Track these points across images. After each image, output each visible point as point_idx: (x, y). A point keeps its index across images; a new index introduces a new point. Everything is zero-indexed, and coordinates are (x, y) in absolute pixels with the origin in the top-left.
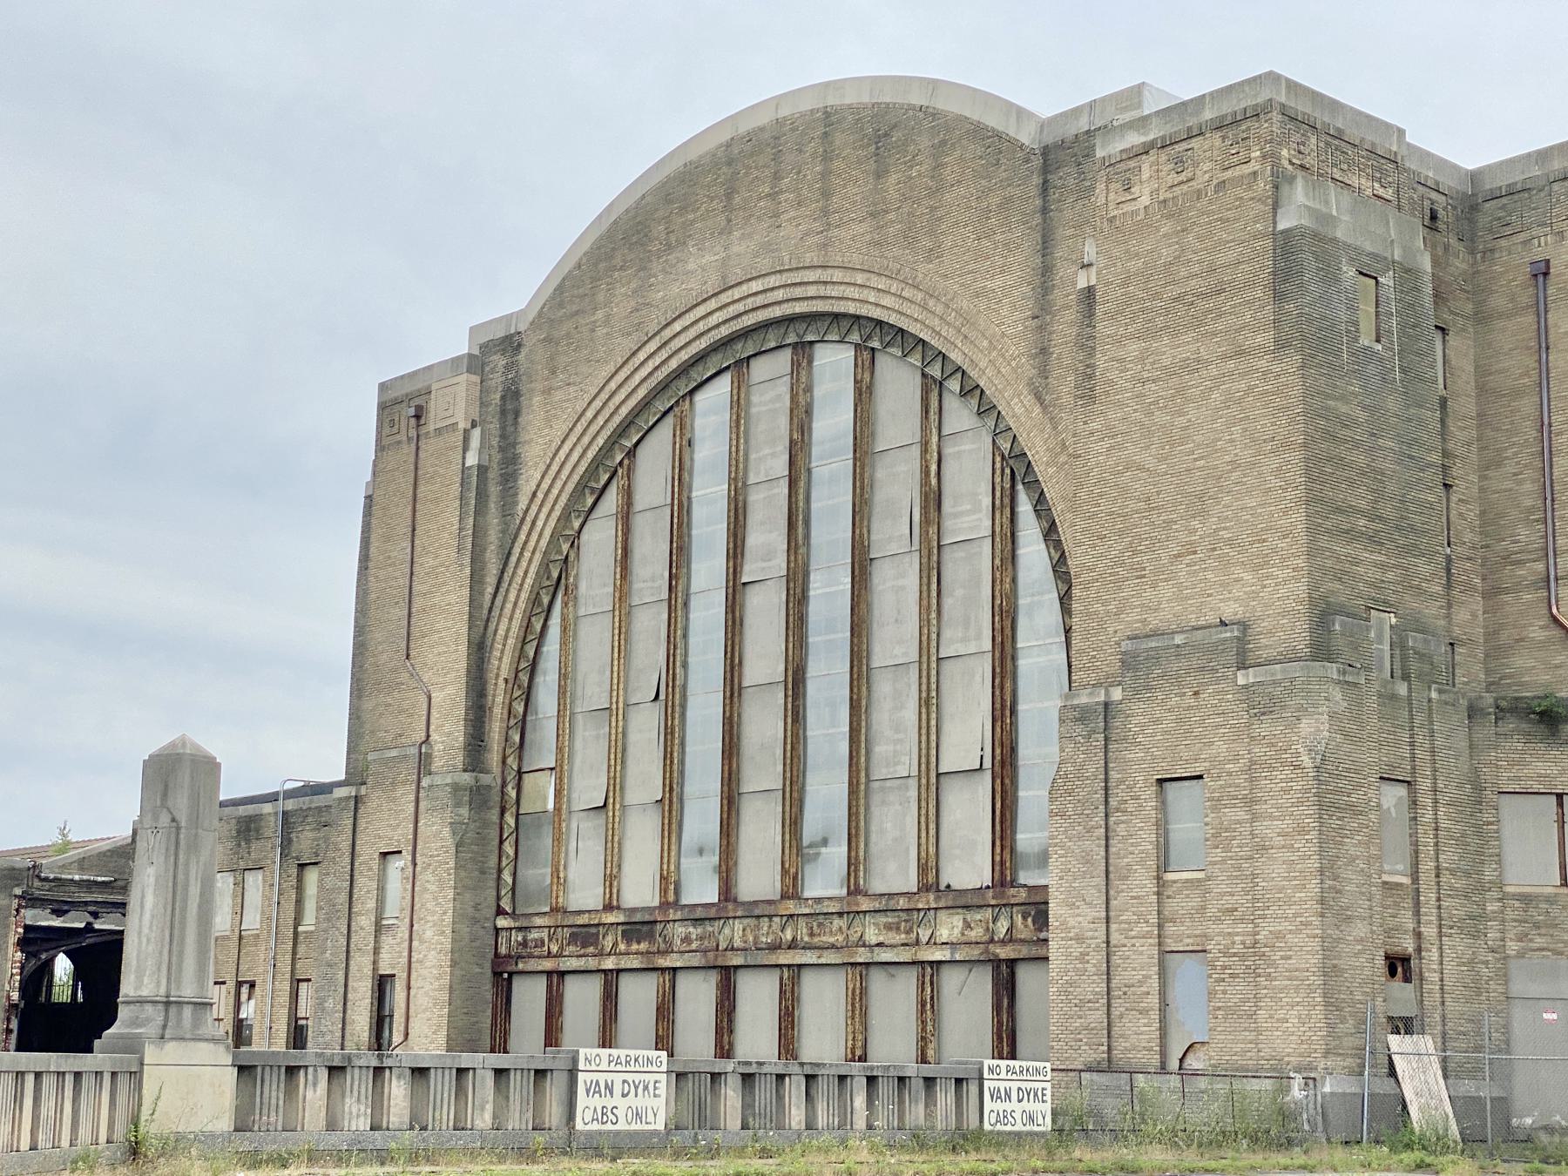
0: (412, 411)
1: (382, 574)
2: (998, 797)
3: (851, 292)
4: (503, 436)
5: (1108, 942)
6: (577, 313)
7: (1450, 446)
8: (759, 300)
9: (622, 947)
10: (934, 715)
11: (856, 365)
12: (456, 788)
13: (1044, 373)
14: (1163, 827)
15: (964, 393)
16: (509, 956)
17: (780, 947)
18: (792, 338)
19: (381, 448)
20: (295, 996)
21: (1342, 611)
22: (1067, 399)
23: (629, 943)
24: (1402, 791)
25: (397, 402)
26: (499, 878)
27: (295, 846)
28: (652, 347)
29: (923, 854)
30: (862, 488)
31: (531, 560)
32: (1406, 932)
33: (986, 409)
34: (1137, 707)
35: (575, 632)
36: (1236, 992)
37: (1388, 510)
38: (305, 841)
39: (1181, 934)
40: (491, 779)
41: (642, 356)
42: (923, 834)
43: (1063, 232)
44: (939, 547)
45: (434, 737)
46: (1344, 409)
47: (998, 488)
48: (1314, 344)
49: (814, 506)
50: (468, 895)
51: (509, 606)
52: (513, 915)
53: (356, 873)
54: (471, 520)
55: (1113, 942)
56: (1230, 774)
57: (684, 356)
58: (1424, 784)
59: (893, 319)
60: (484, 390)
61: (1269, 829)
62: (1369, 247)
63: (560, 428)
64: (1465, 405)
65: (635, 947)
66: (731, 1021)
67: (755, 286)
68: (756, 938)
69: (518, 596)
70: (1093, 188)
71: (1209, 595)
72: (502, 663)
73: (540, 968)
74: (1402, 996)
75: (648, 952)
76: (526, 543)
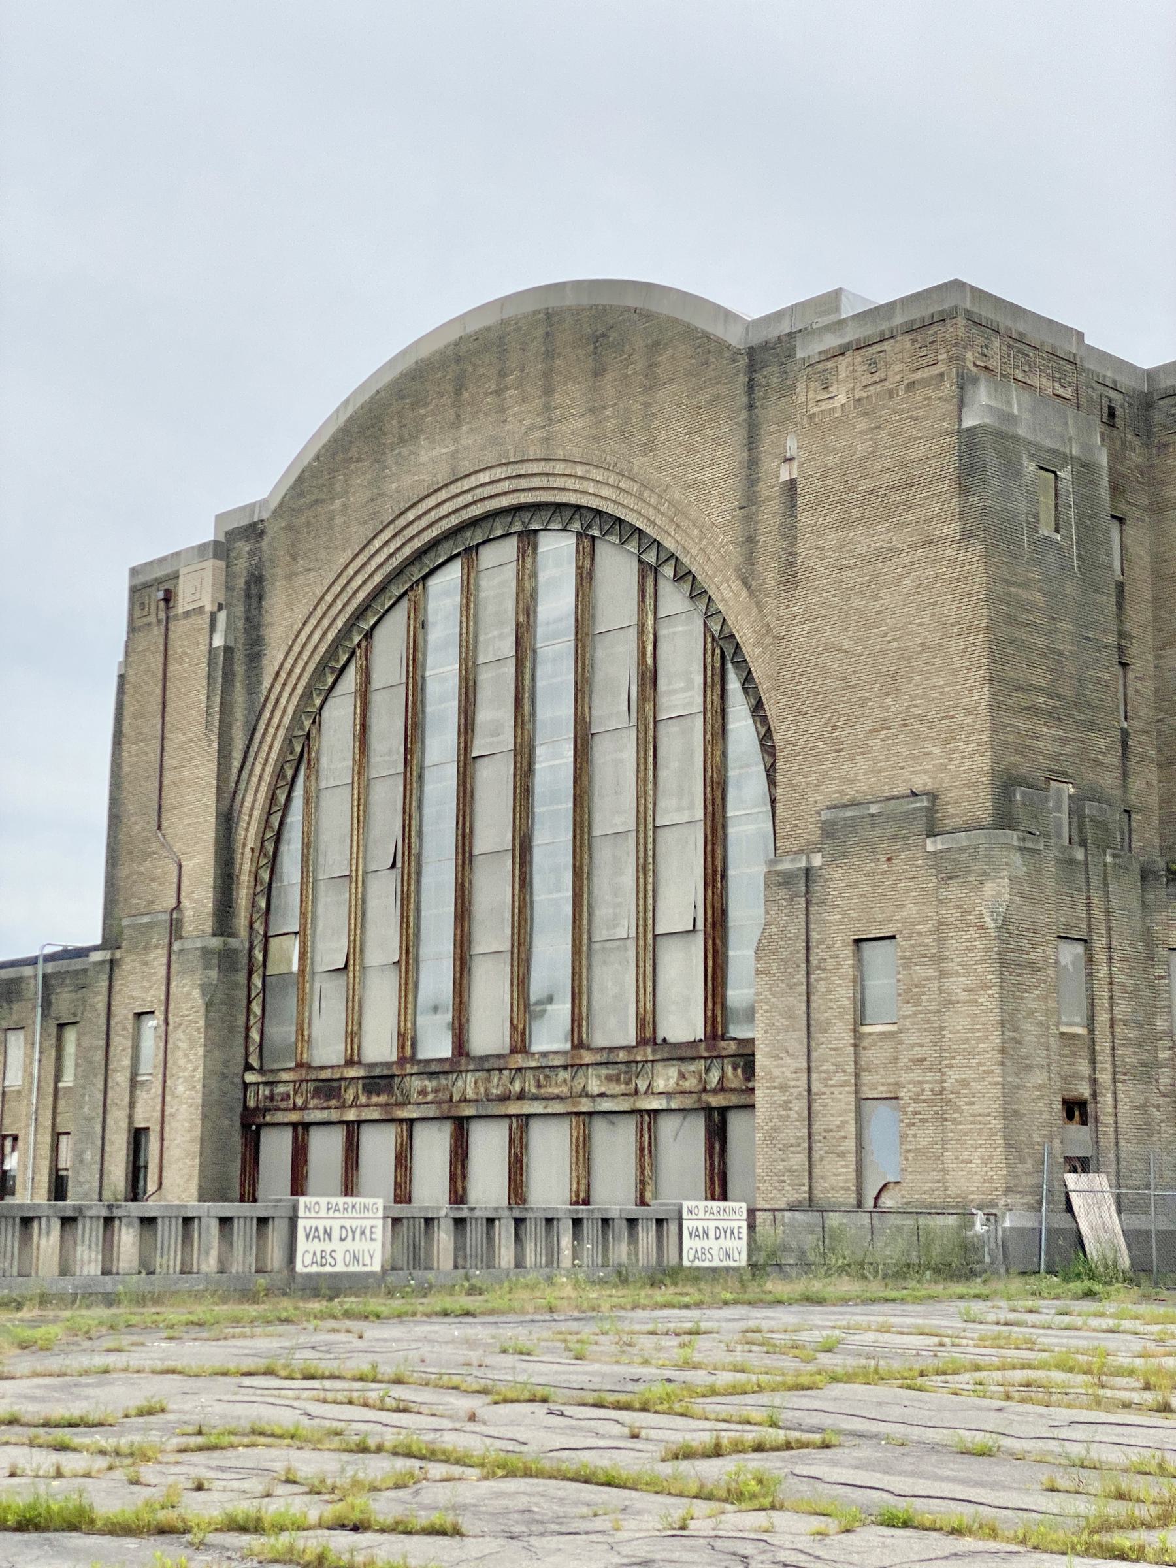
0: (161, 595)
1: (134, 749)
2: (710, 956)
3: (570, 483)
4: (247, 619)
5: (809, 1091)
6: (316, 502)
7: (1128, 627)
8: (487, 491)
9: (363, 1099)
10: (650, 880)
11: (577, 552)
12: (205, 952)
13: (750, 559)
14: (859, 982)
15: (678, 579)
16: (257, 1109)
18: (517, 527)
19: (132, 629)
20: (55, 1149)
21: (1023, 781)
22: (771, 584)
23: (369, 1096)
24: (1079, 948)
25: (147, 586)
26: (247, 1036)
27: (53, 1008)
28: (386, 535)
29: (641, 1011)
30: (584, 669)
31: (275, 735)
32: (1082, 1079)
33: (697, 593)
34: (836, 873)
35: (317, 803)
36: (924, 1136)
37: (1066, 690)
38: (64, 1001)
39: (875, 1083)
40: (239, 943)
41: (377, 544)
43: (769, 429)
44: (655, 722)
45: (185, 903)
46: (1024, 594)
47: (709, 668)
48: (996, 534)
49: (540, 684)
50: (217, 1053)
51: (255, 779)
52: (261, 1071)
53: (112, 1035)
54: (218, 698)
55: (814, 1090)
56: (920, 934)
57: (417, 543)
58: (1100, 942)
59: (610, 509)
60: (230, 575)
61: (956, 985)
62: (1048, 443)
63: (301, 611)
64: (1141, 591)
65: (375, 1099)
66: (464, 1168)
67: (484, 478)
68: (486, 1090)
69: (263, 770)
70: (793, 387)
71: (902, 768)
72: (248, 834)
73: (286, 1120)
74: (1078, 1138)
75: (387, 1105)
76: (270, 719)
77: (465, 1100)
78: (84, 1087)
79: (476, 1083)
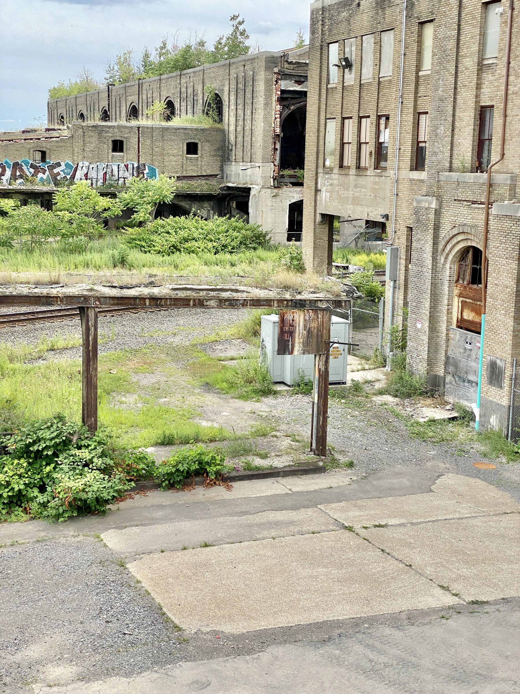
27: (417, 9)
53: (462, 23)
78: (438, 72)
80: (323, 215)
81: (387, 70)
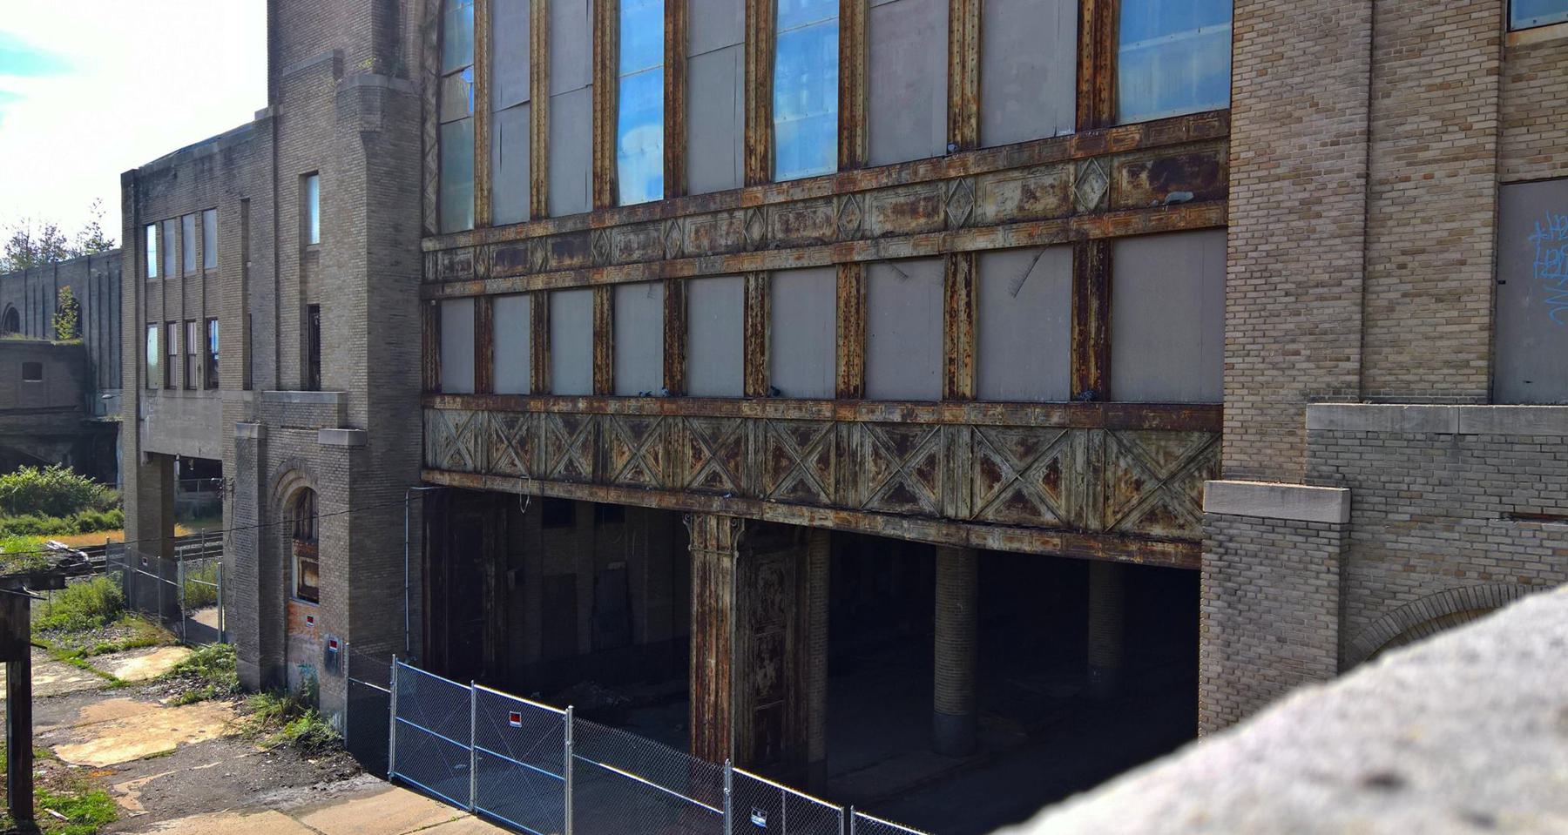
5: (1367, 176)
16: (436, 282)
17: (745, 249)
23: (560, 256)
42: (957, 69)
52: (439, 235)
53: (280, 200)
55: (1379, 173)
65: (567, 262)
66: (683, 345)
73: (467, 292)
77: (683, 256)
79: (697, 231)
80: (151, 455)
81: (213, 262)
